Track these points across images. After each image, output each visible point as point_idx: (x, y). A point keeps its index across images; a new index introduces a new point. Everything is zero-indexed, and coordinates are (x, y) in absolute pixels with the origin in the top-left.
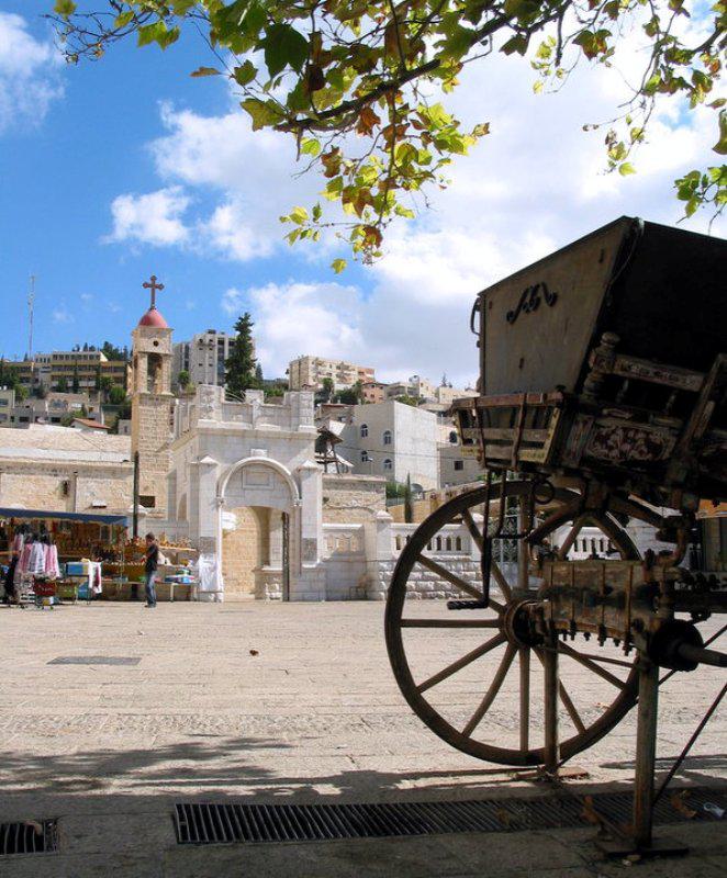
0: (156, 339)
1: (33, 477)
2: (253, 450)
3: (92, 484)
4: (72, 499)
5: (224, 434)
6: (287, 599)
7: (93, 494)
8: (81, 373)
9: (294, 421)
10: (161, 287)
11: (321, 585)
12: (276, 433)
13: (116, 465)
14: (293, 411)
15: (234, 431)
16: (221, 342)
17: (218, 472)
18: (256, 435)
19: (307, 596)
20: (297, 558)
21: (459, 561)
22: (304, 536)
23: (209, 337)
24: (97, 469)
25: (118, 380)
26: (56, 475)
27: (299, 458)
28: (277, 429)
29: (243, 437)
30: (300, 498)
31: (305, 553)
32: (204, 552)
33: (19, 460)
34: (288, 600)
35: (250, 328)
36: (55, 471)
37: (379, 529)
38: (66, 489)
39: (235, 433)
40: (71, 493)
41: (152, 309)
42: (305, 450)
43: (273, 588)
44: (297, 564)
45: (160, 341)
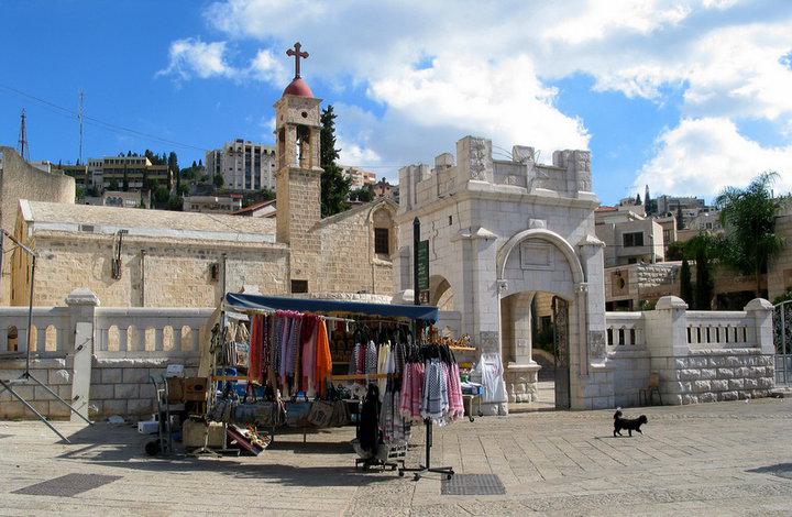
0: (305, 110)
1: (179, 259)
2: (532, 221)
3: (243, 267)
4: (220, 283)
5: (499, 199)
6: (564, 403)
7: (243, 278)
8: (129, 175)
9: (571, 186)
10: (305, 55)
11: (610, 388)
12: (553, 199)
13: (266, 246)
14: (569, 175)
15: (511, 196)
16: (248, 150)
17: (496, 246)
18: (534, 201)
19: (598, 401)
20: (583, 356)
21: (750, 354)
22: (592, 328)
23: (238, 145)
24: (247, 251)
25: (161, 181)
26: (203, 257)
27: (580, 231)
28: (554, 194)
29: (519, 203)
30: (586, 281)
31: (593, 349)
32: (486, 351)
33: (163, 240)
34: (568, 407)
35: (333, 120)
36: (202, 252)
37: (675, 319)
38: (215, 273)
39: (511, 198)
40: (220, 277)
41: (297, 77)
42: (585, 222)
43: (521, 389)
44: (583, 363)
45: (309, 113)
